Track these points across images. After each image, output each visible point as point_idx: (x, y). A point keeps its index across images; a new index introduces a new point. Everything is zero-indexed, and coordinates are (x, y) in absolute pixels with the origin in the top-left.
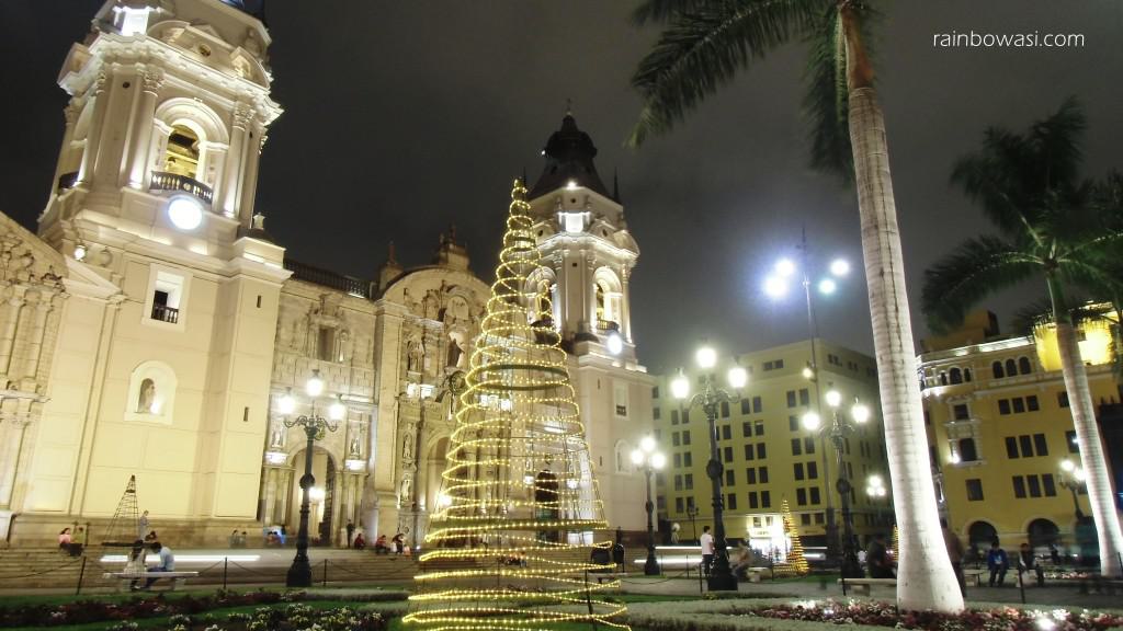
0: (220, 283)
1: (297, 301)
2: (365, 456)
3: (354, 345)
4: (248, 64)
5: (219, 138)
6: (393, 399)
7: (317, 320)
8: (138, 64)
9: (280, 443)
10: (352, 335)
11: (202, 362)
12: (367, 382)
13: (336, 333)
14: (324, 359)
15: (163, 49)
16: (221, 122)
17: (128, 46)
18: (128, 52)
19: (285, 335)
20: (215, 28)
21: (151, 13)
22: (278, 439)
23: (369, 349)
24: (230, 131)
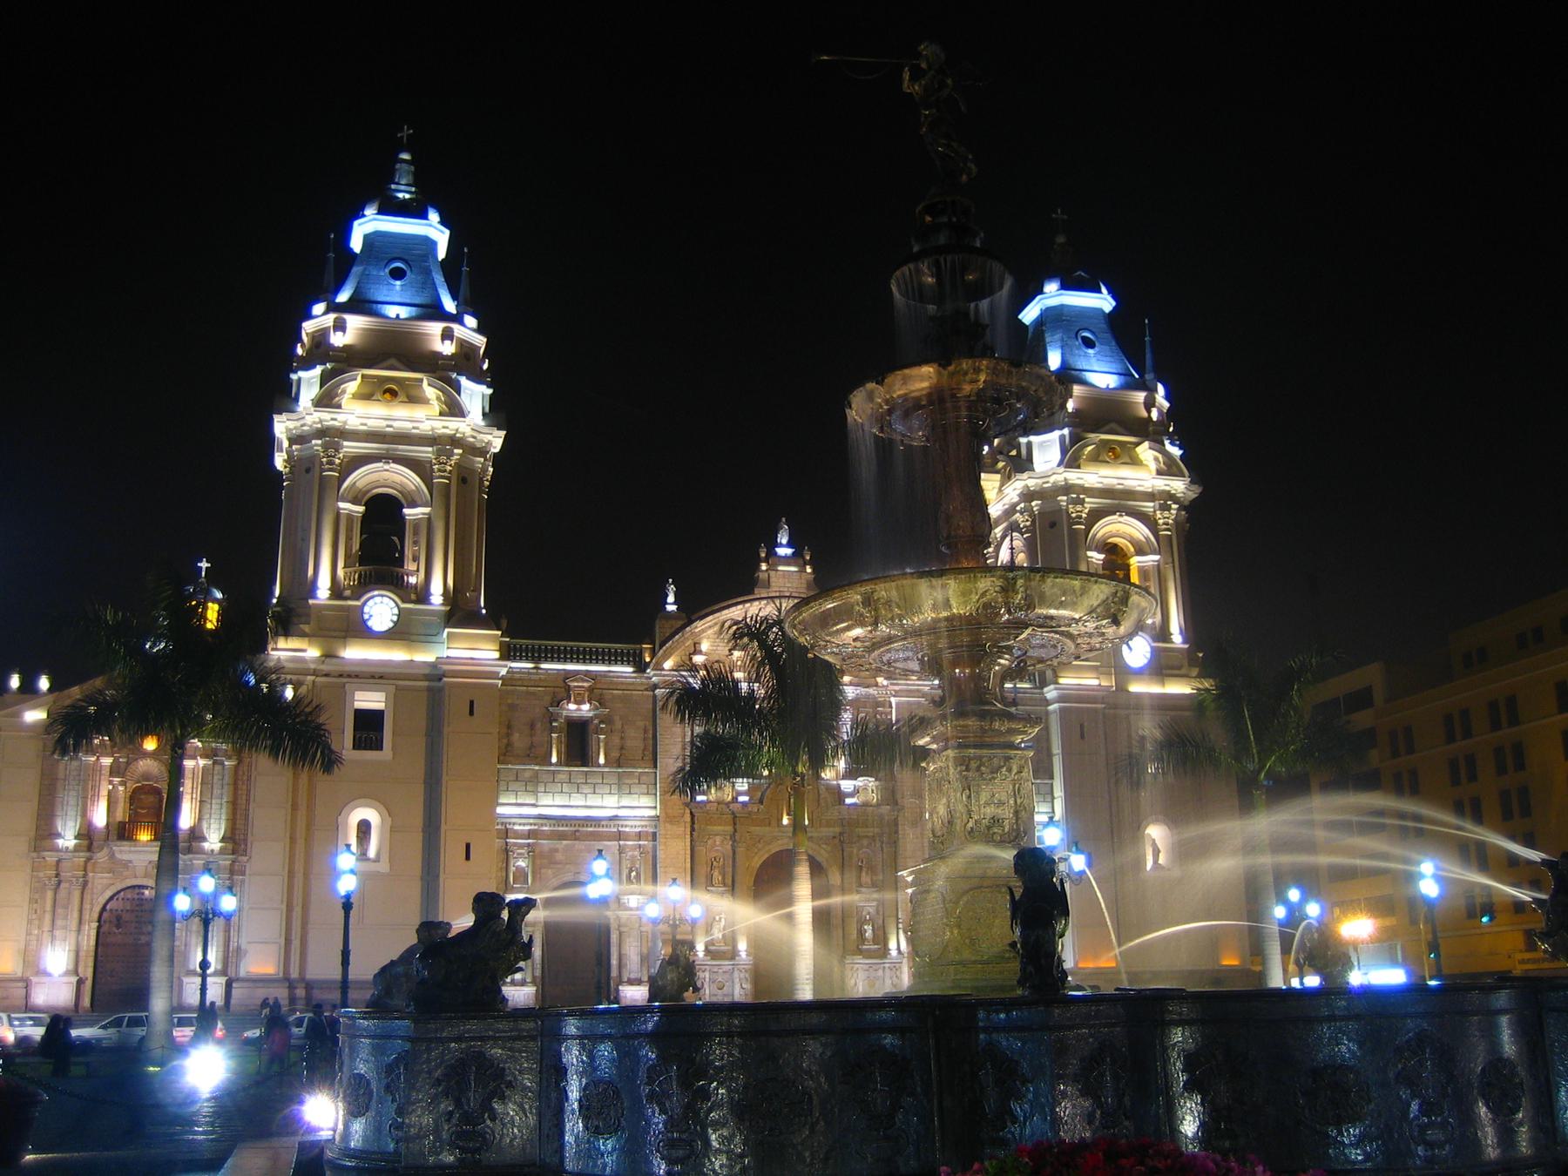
0: (429, 689)
3: (622, 738)
4: (441, 394)
5: (419, 502)
8: (314, 442)
11: (419, 790)
13: (592, 727)
16: (418, 479)
17: (302, 422)
18: (305, 428)
21: (323, 371)
23: (645, 739)
24: (430, 486)
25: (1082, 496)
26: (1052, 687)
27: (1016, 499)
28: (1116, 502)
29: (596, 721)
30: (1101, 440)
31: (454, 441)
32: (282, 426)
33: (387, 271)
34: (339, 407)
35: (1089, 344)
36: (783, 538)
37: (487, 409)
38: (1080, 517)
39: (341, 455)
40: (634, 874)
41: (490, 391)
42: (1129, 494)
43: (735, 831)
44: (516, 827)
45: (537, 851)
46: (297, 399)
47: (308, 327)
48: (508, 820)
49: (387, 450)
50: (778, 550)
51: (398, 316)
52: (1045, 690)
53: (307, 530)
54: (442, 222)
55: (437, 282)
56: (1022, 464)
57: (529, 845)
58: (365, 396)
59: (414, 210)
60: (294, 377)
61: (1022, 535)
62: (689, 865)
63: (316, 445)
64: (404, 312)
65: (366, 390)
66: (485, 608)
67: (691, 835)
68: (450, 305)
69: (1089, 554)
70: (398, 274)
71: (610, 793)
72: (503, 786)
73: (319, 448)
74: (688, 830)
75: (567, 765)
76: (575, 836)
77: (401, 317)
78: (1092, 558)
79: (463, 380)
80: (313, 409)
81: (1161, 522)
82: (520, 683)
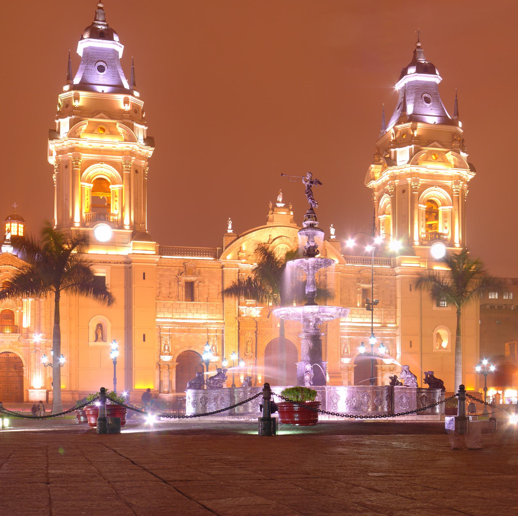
0: (125, 268)
1: (170, 270)
2: (221, 354)
5: (117, 182)
6: (235, 319)
7: (184, 278)
8: (69, 154)
9: (168, 350)
10: (207, 283)
12: (218, 310)
13: (196, 285)
14: (193, 300)
15: (77, 141)
17: (63, 144)
19: (164, 291)
20: (105, 112)
21: (70, 119)
22: (167, 348)
25: (418, 178)
26: (398, 267)
27: (388, 178)
28: (434, 180)
29: (198, 282)
30: (429, 151)
31: (132, 153)
32: (53, 146)
33: (96, 67)
34: (79, 137)
35: (427, 101)
36: (280, 199)
37: (145, 137)
38: (416, 188)
39: (81, 161)
40: (214, 348)
41: (146, 128)
42: (441, 177)
43: (257, 330)
44: (164, 327)
45: (173, 337)
46: (59, 133)
47: (62, 97)
48: (161, 325)
49: (102, 157)
50: (277, 204)
51: (103, 91)
52: (395, 268)
53: (67, 195)
54: (121, 41)
55: (120, 73)
56: (391, 162)
57: (169, 335)
58: (91, 132)
59: (106, 35)
60: (57, 121)
61: (390, 195)
62: (237, 344)
63: (70, 155)
64: (107, 89)
65: (91, 128)
66: (147, 230)
67: (238, 331)
68: (126, 86)
69: (420, 205)
70: (101, 69)
71: (204, 313)
72: (158, 310)
73: (71, 157)
74: (237, 329)
75: (185, 301)
76: (189, 331)
77: (105, 92)
78: (421, 207)
79: (135, 124)
80: (67, 138)
81: (454, 190)
82: (164, 265)
